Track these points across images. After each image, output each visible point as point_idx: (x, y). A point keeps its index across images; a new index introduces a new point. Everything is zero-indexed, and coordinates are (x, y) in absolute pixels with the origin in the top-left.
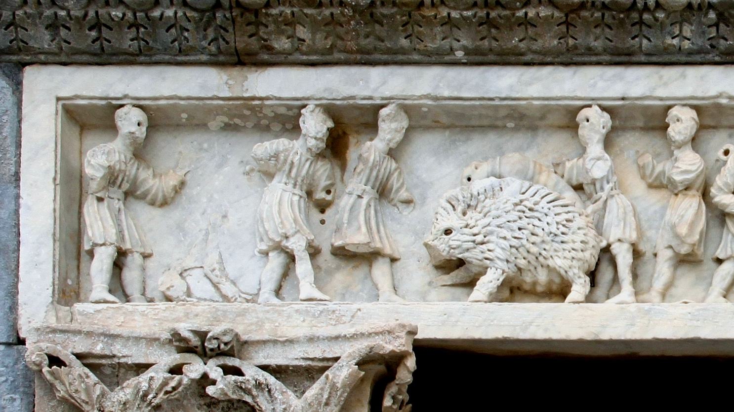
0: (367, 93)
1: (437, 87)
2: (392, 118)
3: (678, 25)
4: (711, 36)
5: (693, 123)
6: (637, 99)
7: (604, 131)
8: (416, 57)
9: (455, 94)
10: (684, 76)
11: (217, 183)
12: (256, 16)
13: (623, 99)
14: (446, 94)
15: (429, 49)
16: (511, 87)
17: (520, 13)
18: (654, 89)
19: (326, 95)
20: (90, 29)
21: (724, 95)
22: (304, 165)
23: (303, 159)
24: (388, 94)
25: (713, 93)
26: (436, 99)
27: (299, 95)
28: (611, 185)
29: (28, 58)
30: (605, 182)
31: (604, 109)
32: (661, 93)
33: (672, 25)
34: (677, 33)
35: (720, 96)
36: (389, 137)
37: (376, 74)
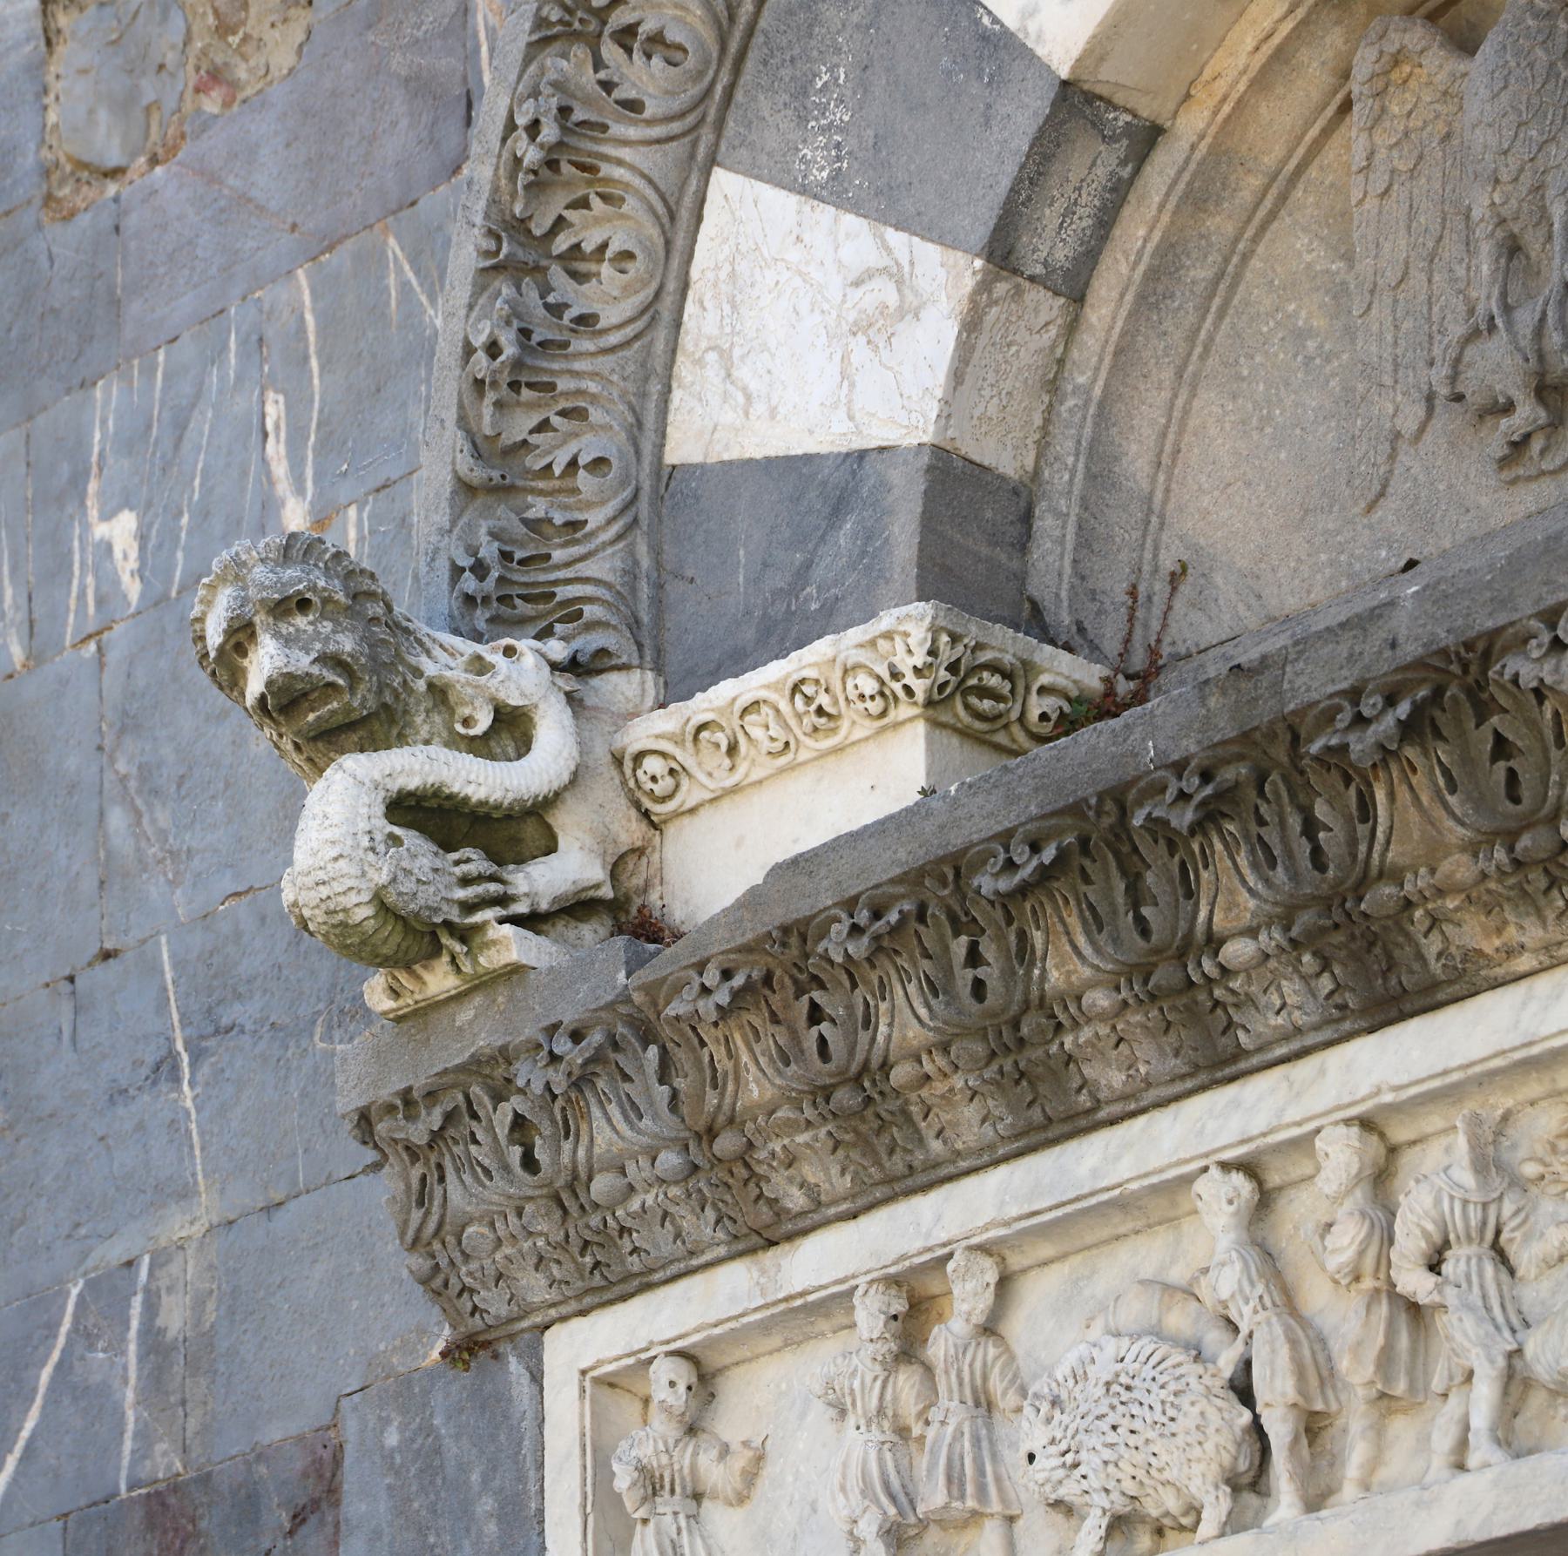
0: (919, 1244)
1: (1003, 1203)
2: (966, 1274)
3: (1272, 989)
4: (1327, 991)
5: (1348, 1152)
6: (1264, 1135)
7: (1232, 1209)
8: (963, 1164)
9: (1027, 1209)
10: (1322, 1072)
11: (801, 1446)
12: (747, 1165)
13: (1243, 1142)
14: (1014, 1211)
15: (972, 1145)
16: (1095, 1173)
17: (1054, 1048)
18: (1283, 1110)
19: (872, 1264)
20: (582, 1256)
21: (1384, 1087)
22: (871, 1389)
23: (868, 1379)
24: (944, 1237)
25: (1364, 1091)
26: (1007, 1224)
27: (841, 1275)
28: (1252, 1304)
29: (538, 1319)
30: (1241, 1303)
31: (1225, 1166)
32: (1293, 1114)
33: (1265, 991)
34: (1278, 1003)
35: (1378, 1092)
36: (965, 1307)
37: (924, 1207)
